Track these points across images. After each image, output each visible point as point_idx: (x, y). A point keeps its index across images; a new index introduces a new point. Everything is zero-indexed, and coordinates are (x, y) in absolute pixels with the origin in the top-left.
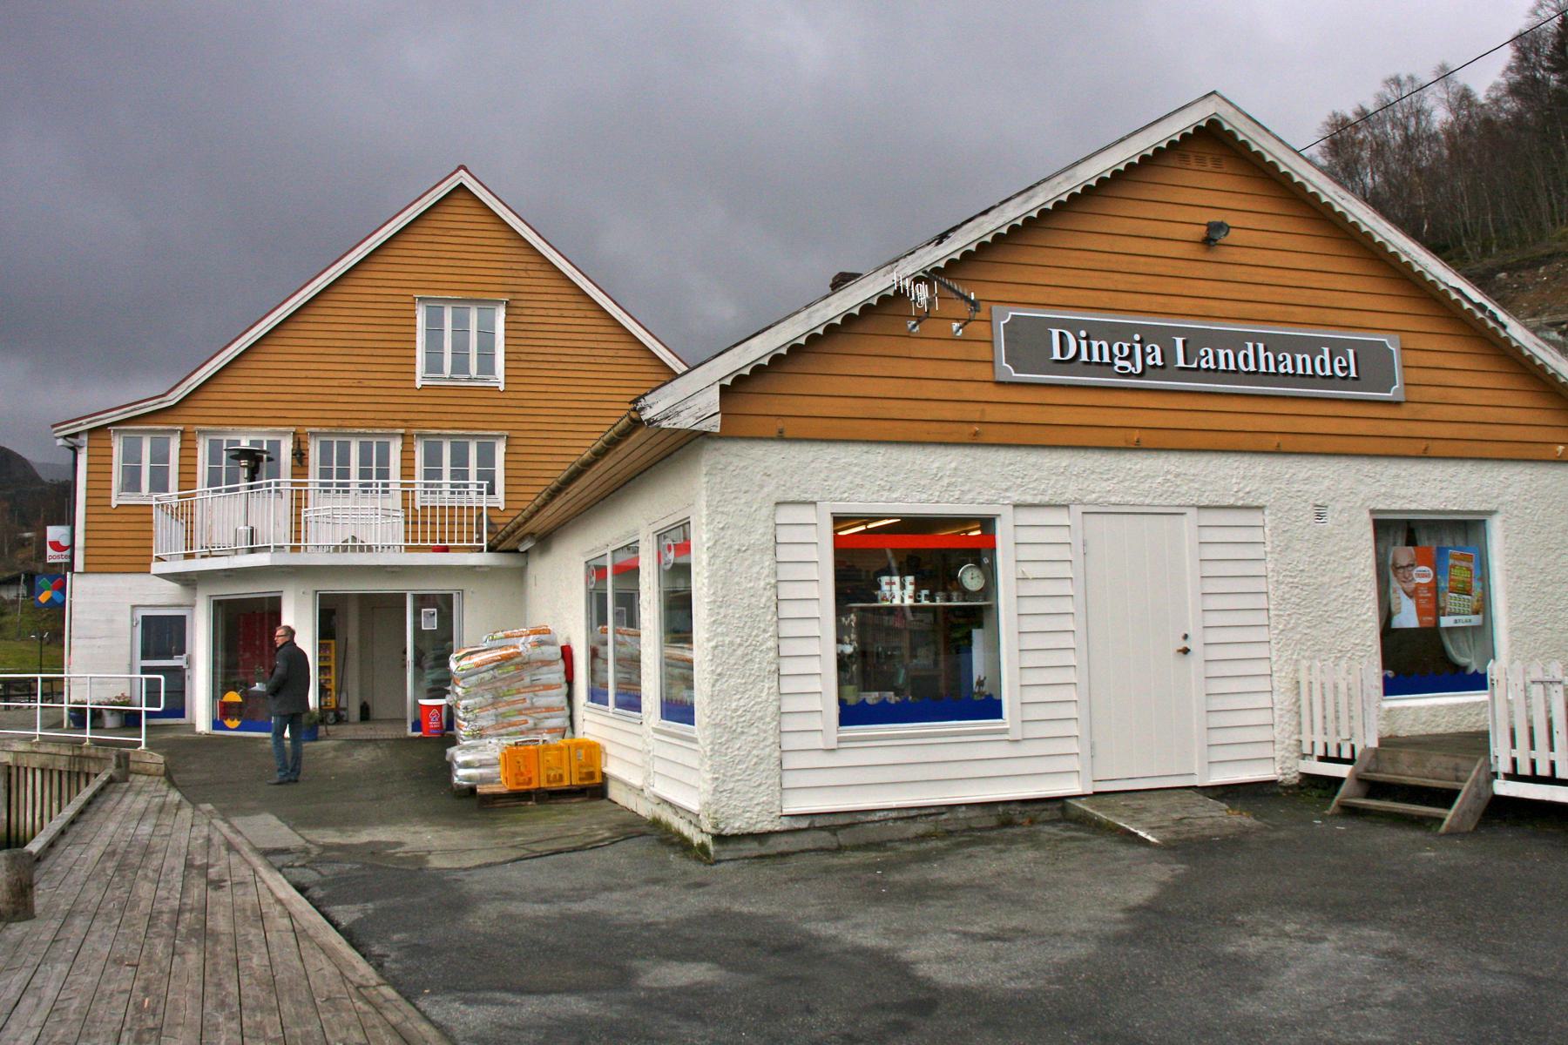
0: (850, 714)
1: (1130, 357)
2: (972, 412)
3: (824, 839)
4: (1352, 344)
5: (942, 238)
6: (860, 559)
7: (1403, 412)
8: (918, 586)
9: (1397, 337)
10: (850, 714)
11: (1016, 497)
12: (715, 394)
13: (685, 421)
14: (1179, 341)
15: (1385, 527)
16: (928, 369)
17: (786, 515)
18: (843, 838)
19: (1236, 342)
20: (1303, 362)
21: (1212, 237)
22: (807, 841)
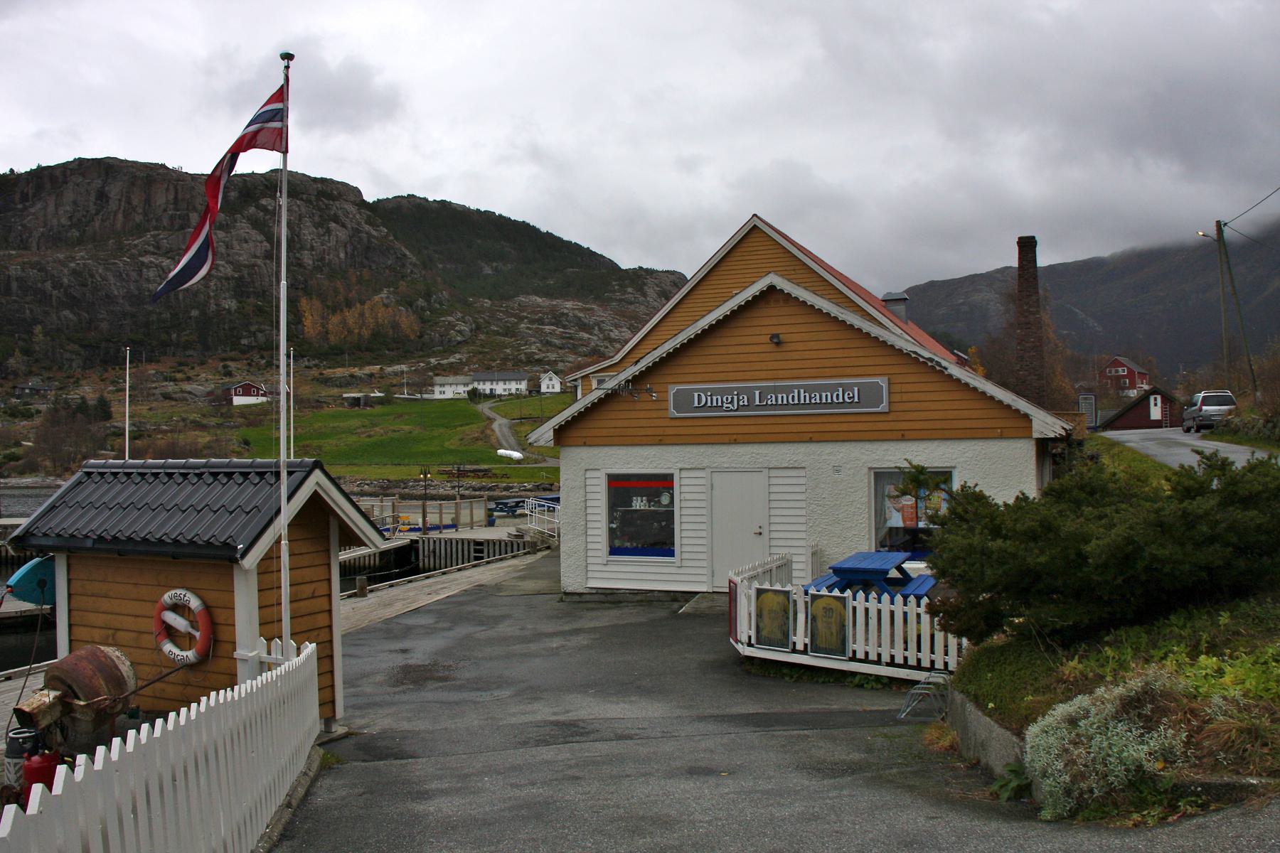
0: (614, 551)
1: (732, 402)
2: (660, 431)
3: (602, 598)
4: (855, 385)
5: (637, 362)
6: (621, 487)
7: (890, 417)
8: (649, 501)
9: (886, 379)
10: (614, 551)
11: (680, 466)
12: (551, 433)
13: (542, 443)
14: (757, 393)
15: (880, 476)
16: (642, 414)
17: (589, 474)
18: (609, 598)
19: (789, 390)
20: (826, 397)
21: (777, 341)
22: (596, 598)
